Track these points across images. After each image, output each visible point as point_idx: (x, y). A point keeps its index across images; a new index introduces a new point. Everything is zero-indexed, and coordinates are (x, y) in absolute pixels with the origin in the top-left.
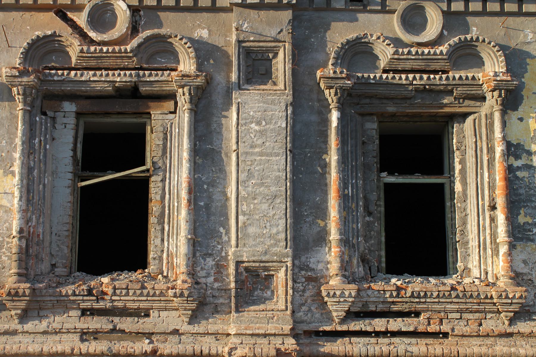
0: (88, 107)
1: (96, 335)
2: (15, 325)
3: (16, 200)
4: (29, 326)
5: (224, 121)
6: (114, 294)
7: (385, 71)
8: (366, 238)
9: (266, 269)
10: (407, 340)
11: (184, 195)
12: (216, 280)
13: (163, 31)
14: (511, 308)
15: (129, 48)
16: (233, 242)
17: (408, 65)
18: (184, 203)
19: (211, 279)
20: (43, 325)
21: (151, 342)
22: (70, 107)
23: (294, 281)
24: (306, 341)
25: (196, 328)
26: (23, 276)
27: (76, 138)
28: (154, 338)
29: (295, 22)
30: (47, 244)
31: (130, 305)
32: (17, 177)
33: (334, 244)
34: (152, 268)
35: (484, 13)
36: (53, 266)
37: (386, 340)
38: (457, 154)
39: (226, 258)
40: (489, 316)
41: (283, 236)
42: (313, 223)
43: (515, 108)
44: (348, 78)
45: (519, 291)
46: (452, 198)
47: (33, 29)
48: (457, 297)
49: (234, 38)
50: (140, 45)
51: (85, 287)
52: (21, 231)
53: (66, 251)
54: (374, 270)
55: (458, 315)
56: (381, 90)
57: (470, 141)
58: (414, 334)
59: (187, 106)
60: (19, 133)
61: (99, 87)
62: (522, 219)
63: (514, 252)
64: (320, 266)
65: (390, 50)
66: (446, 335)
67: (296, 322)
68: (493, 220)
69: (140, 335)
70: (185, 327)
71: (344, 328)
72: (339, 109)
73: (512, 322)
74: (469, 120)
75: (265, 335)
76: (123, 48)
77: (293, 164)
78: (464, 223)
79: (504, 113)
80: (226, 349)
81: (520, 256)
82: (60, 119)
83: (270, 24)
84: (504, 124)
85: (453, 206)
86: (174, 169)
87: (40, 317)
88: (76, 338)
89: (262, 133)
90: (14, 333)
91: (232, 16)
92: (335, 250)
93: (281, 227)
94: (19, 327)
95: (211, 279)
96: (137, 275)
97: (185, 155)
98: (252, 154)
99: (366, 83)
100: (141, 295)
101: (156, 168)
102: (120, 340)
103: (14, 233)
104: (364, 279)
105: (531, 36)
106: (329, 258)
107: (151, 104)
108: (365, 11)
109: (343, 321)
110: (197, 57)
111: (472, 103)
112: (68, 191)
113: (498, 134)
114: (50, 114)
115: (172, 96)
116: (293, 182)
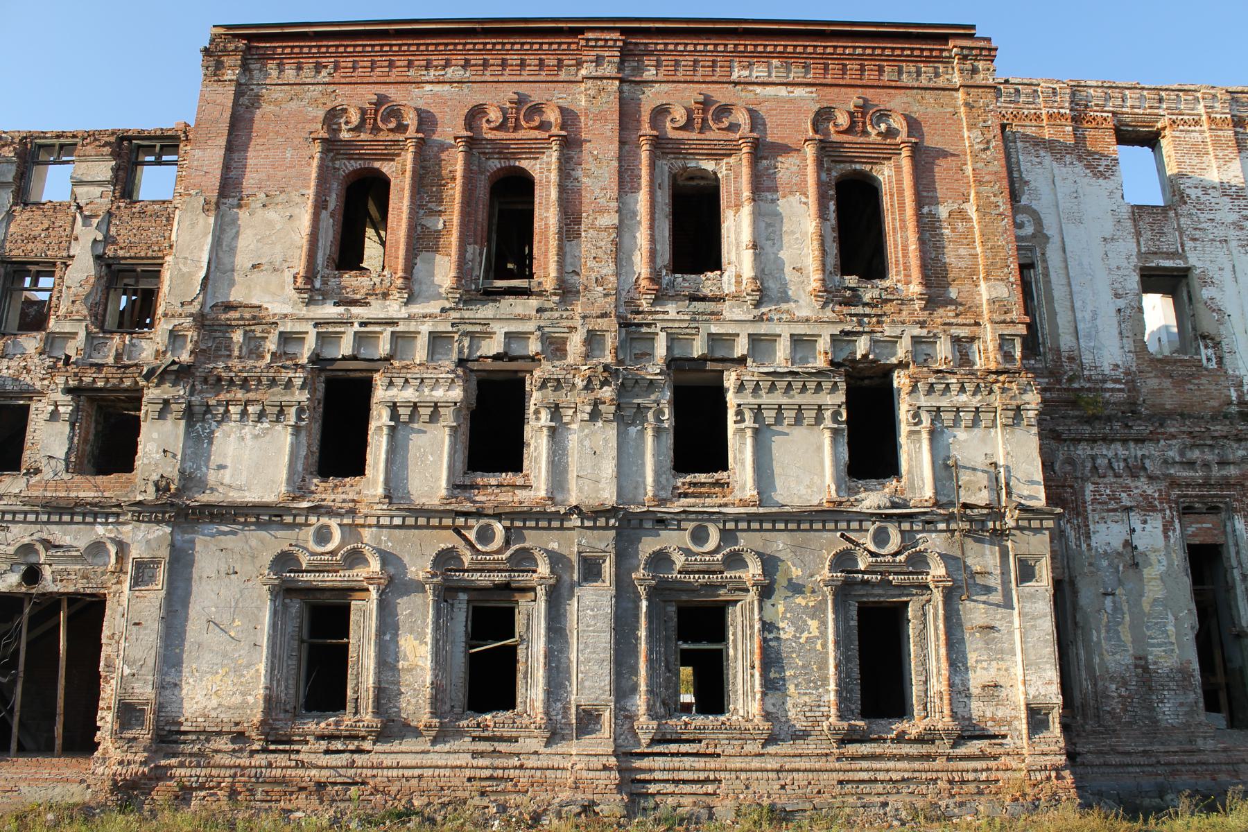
0: (475, 595)
1: (482, 754)
2: (428, 747)
3: (429, 662)
4: (438, 748)
5: (568, 607)
6: (495, 727)
7: (680, 572)
8: (667, 688)
9: (597, 710)
10: (692, 759)
12: (563, 718)
13: (527, 545)
14: (762, 737)
15: (504, 557)
16: (575, 692)
17: (696, 568)
18: (542, 664)
19: (560, 717)
20: (447, 747)
21: (519, 760)
22: (463, 597)
23: (616, 718)
24: (623, 759)
25: (549, 750)
26: (434, 714)
27: (467, 617)
28: (521, 757)
29: (618, 539)
30: (448, 691)
31: (504, 734)
32: (429, 646)
33: (642, 693)
34: (519, 709)
35: (749, 529)
36: (453, 707)
37: (678, 759)
38: (731, 628)
39: (569, 703)
40: (748, 742)
41: (608, 688)
42: (630, 678)
43: (769, 597)
44: (653, 579)
45: (767, 725)
46: (728, 660)
47: (439, 542)
48: (726, 729)
49: (576, 550)
50: (511, 555)
51: (475, 722)
52: (432, 683)
53: (461, 696)
54: (672, 710)
55: (727, 742)
56: (677, 586)
57: (739, 619)
58: (697, 755)
59: (543, 598)
60: (431, 616)
61: (483, 584)
62: (772, 675)
63: (766, 698)
64: (634, 708)
65: (683, 558)
66: (719, 755)
67: (616, 746)
68: (752, 676)
69: (512, 755)
70: (542, 750)
71: (649, 750)
72: (647, 599)
73: (764, 746)
74: (739, 604)
75: (596, 755)
76: (500, 556)
77: (615, 636)
78: (735, 677)
79: (761, 602)
80: (570, 765)
81: (770, 700)
82: (457, 605)
83: (600, 540)
84: (761, 609)
85: (728, 665)
86: (535, 641)
87: (445, 742)
88: (469, 756)
89: (594, 617)
90: (428, 752)
91: (575, 533)
92: (644, 697)
93: (607, 682)
94: (431, 749)
95: (560, 717)
96: (509, 714)
97: (543, 632)
98: (588, 631)
99: (666, 580)
100: (513, 727)
101: (522, 640)
102: (499, 758)
103: (428, 685)
104: (664, 717)
105: (781, 545)
106: (639, 702)
107: (516, 594)
108: (666, 529)
109: (649, 746)
110: (551, 563)
111: (740, 593)
112: (463, 655)
113: (756, 617)
114: (450, 601)
115: (533, 589)
116: (616, 650)
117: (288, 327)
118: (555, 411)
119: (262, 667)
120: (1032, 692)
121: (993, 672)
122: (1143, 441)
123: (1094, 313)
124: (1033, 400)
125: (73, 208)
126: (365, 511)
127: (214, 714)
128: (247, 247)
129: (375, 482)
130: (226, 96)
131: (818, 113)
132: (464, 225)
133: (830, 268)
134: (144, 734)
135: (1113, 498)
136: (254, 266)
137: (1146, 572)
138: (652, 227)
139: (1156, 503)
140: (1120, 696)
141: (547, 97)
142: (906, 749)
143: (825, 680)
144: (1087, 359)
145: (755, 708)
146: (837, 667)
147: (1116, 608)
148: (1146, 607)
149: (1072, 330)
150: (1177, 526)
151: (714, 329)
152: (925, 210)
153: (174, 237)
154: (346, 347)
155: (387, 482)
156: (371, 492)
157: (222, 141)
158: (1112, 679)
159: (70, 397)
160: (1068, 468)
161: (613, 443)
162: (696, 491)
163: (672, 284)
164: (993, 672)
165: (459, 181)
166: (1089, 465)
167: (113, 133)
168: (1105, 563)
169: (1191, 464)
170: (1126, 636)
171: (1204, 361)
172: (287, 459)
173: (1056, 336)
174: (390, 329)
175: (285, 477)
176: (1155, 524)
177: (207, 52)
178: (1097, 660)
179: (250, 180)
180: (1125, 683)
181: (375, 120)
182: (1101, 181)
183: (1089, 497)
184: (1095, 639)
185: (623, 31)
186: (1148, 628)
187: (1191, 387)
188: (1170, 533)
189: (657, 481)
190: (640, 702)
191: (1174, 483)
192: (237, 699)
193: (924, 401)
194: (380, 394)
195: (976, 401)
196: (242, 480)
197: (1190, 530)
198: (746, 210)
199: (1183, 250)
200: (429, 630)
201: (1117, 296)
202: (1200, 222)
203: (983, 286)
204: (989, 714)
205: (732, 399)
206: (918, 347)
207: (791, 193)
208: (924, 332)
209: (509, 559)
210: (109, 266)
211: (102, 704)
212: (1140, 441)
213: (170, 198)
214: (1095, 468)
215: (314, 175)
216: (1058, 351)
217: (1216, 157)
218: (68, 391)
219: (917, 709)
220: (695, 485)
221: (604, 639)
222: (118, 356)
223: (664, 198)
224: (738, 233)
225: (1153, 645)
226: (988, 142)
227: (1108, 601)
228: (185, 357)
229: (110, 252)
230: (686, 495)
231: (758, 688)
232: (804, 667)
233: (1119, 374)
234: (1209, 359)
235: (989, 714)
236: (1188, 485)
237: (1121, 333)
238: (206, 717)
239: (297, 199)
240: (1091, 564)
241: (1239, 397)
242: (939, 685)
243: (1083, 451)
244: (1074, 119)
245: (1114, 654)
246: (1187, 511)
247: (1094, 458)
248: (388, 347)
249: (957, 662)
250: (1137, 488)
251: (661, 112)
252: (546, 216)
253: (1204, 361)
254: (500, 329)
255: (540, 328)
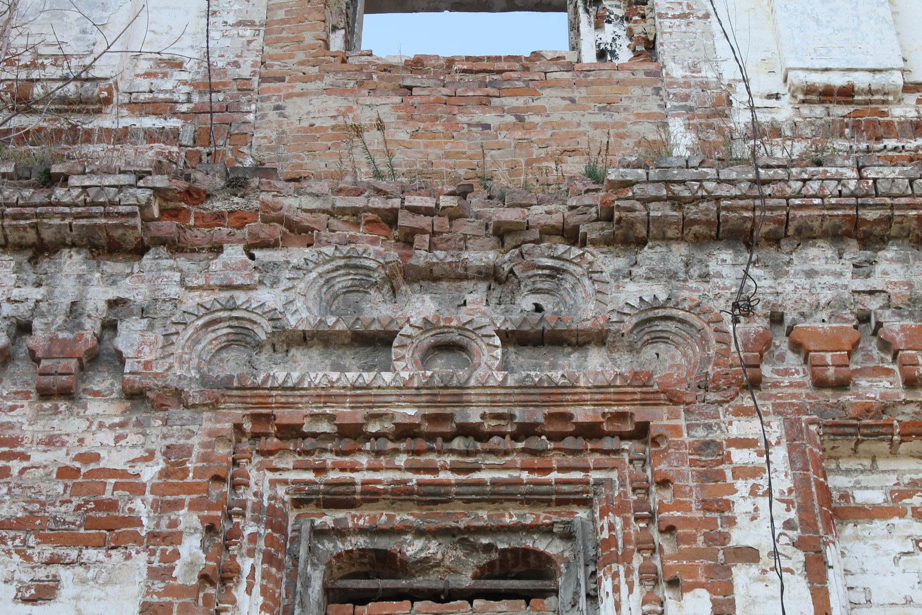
139: (141, 507)
187: (490, 118)
250: (51, 442)
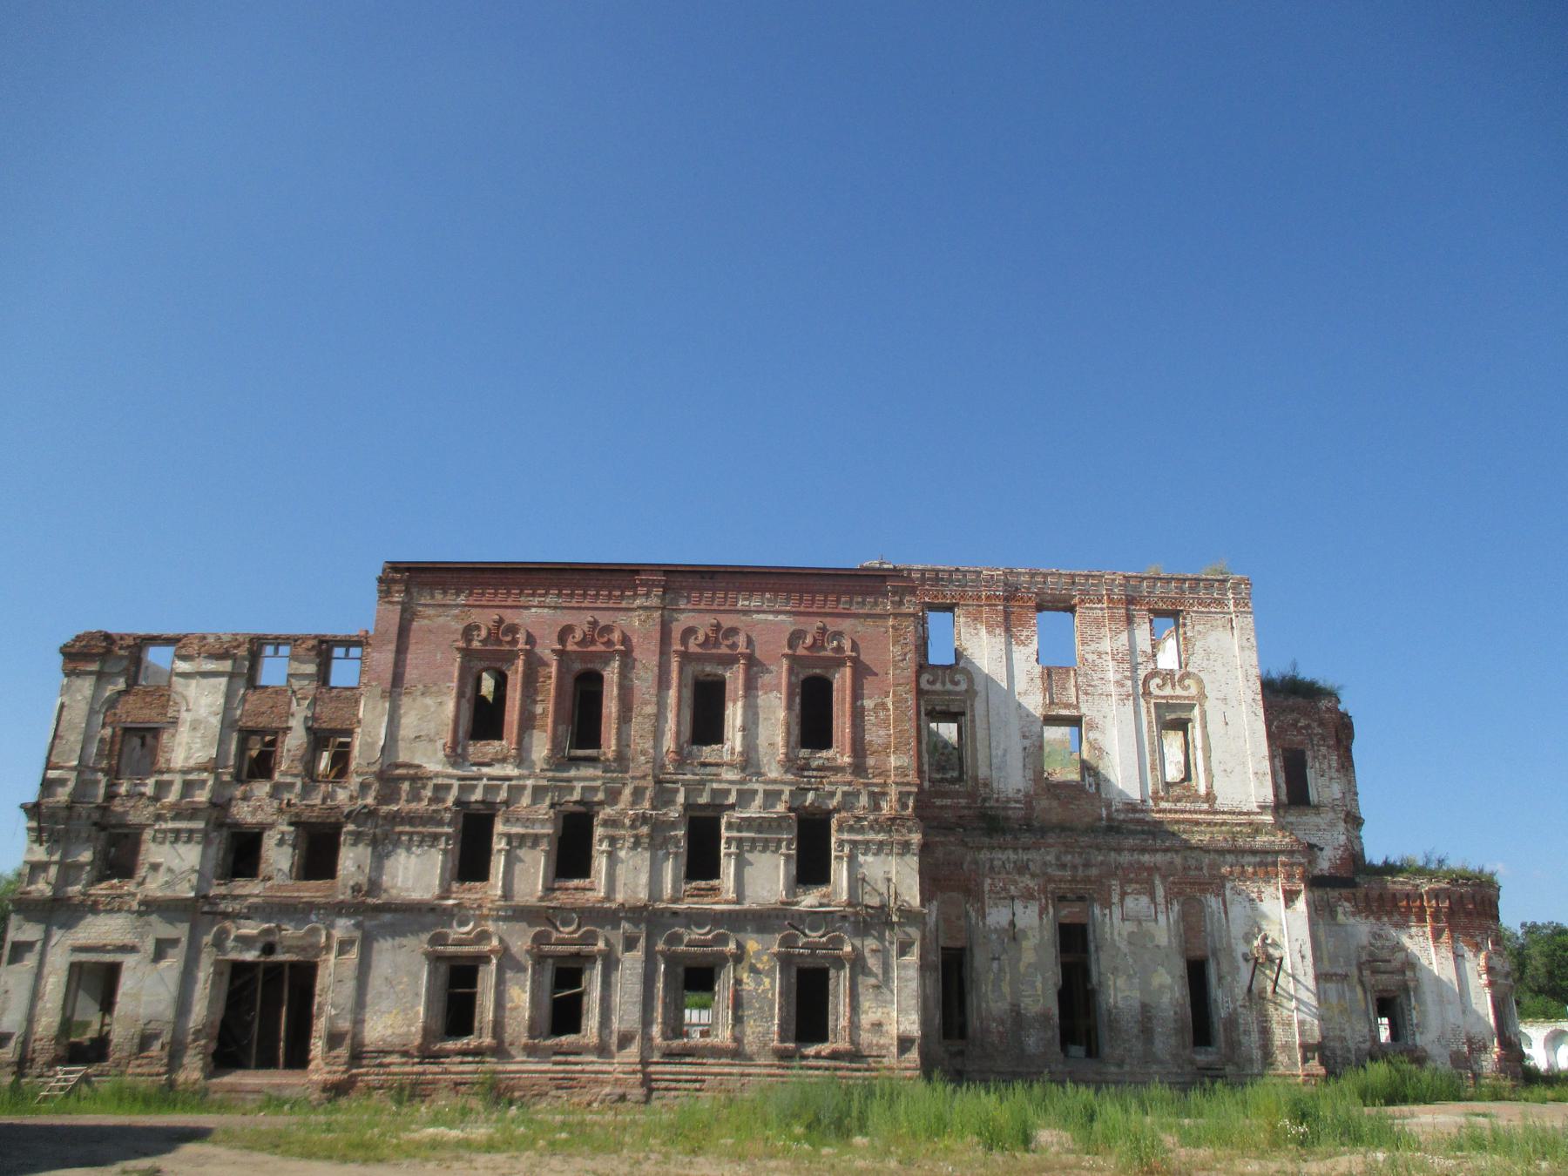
8: (675, 1021)
11: (598, 1001)
34: (583, 1033)
81: (737, 1029)
89: (631, 975)
117: (440, 781)
118: (613, 841)
119: (421, 1009)
120: (902, 1028)
121: (879, 1014)
122: (1029, 849)
123: (1005, 751)
124: (916, 838)
125: (290, 693)
126: (490, 905)
127: (389, 1039)
128: (409, 723)
129: (495, 886)
130: (394, 614)
131: (792, 634)
132: (556, 711)
133: (792, 744)
134: (343, 1052)
135: (1004, 889)
136: (416, 737)
137: (1025, 944)
138: (678, 715)
140: (999, 1032)
141: (613, 619)
142: (821, 1063)
143: (773, 1017)
144: (995, 785)
145: (728, 1033)
146: (780, 1009)
147: (1001, 969)
148: (1022, 969)
149: (988, 763)
150: (1051, 910)
151: (715, 786)
152: (859, 703)
153: (361, 715)
154: (477, 796)
155: (504, 885)
156: (493, 893)
157: (393, 647)
158: (994, 1020)
159: (292, 829)
160: (974, 867)
161: (648, 863)
162: (700, 893)
163: (690, 753)
164: (879, 1014)
165: (553, 680)
166: (987, 866)
167: (316, 637)
168: (994, 937)
169: (1063, 866)
170: (1006, 989)
171: (1087, 786)
172: (439, 871)
173: (975, 766)
174: (507, 783)
175: (437, 882)
176: (1034, 909)
177: (380, 580)
178: (984, 1005)
179: (411, 674)
180: (1002, 1022)
181: (498, 634)
182: (1021, 648)
183: (987, 888)
184: (984, 990)
185: (666, 573)
186: (1022, 984)
187: (1072, 806)
188: (1044, 916)
189: (674, 887)
190: (656, 1030)
191: (1050, 879)
192: (404, 1029)
193: (846, 836)
194: (499, 827)
195: (881, 837)
196: (410, 884)
197: (1064, 912)
198: (740, 704)
199: (1078, 702)
200: (528, 983)
201: (1024, 737)
202: (1093, 680)
203: (892, 758)
204: (874, 1042)
205: (724, 834)
206: (847, 798)
207: (771, 691)
208: (851, 789)
209: (581, 936)
210: (315, 734)
211: (314, 1034)
212: (1026, 849)
213: (355, 685)
214: (992, 868)
215: (456, 674)
216: (976, 778)
217: (1110, 630)
218: (291, 824)
219: (831, 1037)
220: (699, 889)
221: (637, 988)
222: (324, 800)
223: (688, 694)
224: (734, 720)
225: (1025, 996)
226: (905, 654)
227: (995, 965)
228: (370, 800)
229: (316, 726)
230: (692, 896)
231: (730, 1021)
232: (760, 1008)
233: (1020, 796)
234: (1090, 785)
235: (874, 1042)
236: (1060, 881)
237: (1024, 766)
238: (384, 1041)
239: (445, 690)
240: (984, 937)
241: (1108, 815)
242: (843, 1022)
243: (984, 856)
244: (1006, 599)
245: (997, 1002)
246: (1062, 899)
247: (992, 860)
248: (506, 795)
249: (855, 1007)
251: (689, 632)
252: (610, 707)
253: (1087, 786)
254: (579, 785)
255: (604, 784)
